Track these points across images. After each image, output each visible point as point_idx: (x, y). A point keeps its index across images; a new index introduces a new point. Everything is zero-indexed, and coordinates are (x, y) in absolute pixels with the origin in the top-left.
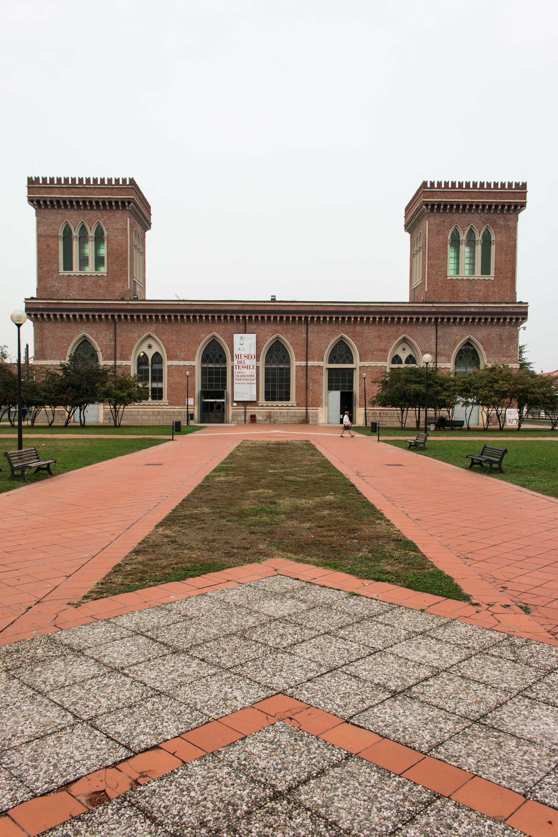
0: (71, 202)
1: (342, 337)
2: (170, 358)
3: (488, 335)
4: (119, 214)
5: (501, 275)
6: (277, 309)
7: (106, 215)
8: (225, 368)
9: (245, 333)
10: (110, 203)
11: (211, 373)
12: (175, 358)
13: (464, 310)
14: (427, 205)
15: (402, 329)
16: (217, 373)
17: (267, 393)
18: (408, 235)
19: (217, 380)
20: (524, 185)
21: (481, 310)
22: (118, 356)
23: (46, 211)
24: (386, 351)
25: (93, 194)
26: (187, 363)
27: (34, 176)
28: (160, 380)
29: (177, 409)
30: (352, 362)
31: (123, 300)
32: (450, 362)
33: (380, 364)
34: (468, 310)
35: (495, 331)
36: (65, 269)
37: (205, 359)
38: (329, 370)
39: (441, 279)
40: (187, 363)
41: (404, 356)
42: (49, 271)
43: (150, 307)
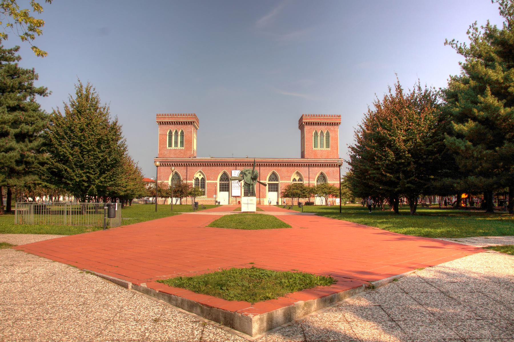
0: (172, 122)
1: (273, 171)
2: (208, 180)
3: (329, 171)
4: (189, 126)
5: (333, 148)
6: (248, 161)
7: (185, 126)
8: (229, 183)
9: (236, 170)
10: (186, 122)
11: (223, 185)
12: (210, 180)
13: (319, 161)
14: (304, 123)
15: (296, 168)
16: (225, 185)
17: (245, 193)
18: (300, 131)
19: (225, 188)
20: (340, 116)
21: (325, 161)
22: (188, 178)
23: (163, 126)
24: (290, 177)
25: (180, 119)
26: (214, 182)
27: (159, 113)
28: (204, 187)
29: (210, 199)
30: (277, 181)
31: (190, 158)
32: (314, 181)
33: (288, 182)
34: (321, 161)
35: (331, 169)
36: (169, 146)
37: (221, 180)
38: (268, 184)
39: (311, 149)
40: (214, 182)
41: (297, 178)
42: (163, 148)
43: (200, 161)
